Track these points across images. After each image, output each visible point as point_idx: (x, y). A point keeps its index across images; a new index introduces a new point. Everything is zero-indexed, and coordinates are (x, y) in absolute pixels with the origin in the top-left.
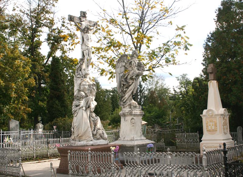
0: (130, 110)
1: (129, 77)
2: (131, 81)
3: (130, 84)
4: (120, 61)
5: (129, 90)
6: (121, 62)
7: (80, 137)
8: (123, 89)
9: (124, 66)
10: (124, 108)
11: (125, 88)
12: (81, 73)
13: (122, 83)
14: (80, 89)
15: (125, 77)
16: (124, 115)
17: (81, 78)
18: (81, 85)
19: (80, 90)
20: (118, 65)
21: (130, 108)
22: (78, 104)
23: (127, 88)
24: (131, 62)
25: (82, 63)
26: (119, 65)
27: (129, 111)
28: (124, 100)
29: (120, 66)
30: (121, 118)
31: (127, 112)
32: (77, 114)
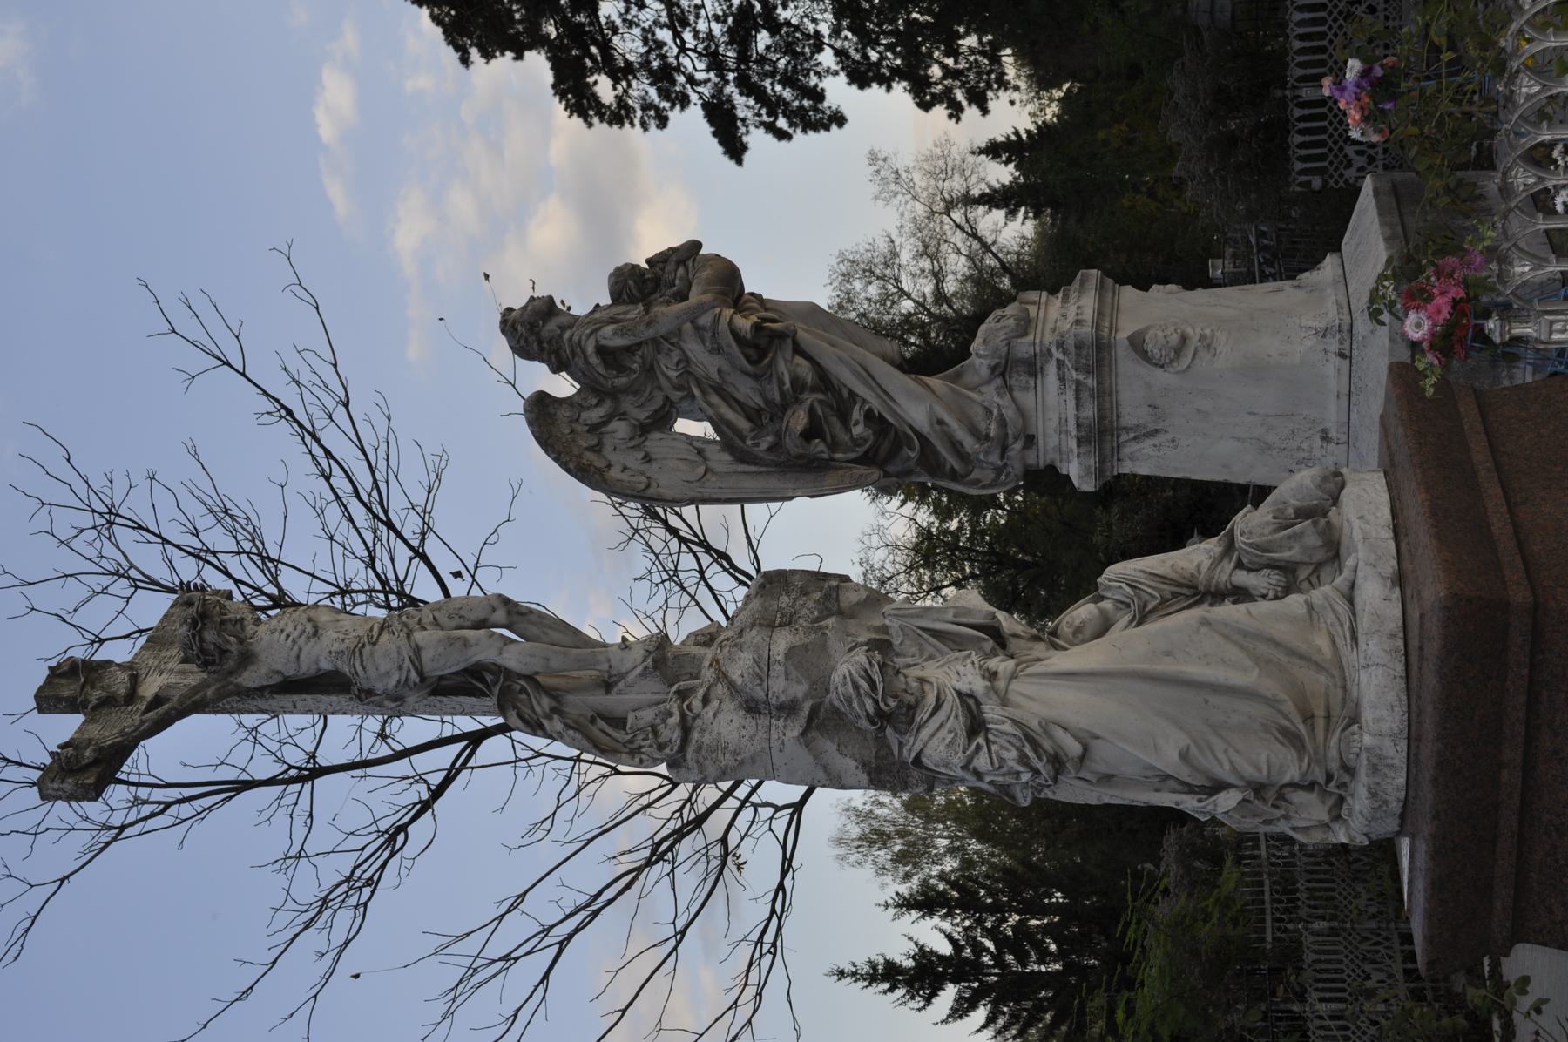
0: (1051, 369)
1: (746, 389)
2: (782, 366)
3: (804, 369)
4: (590, 456)
5: (861, 390)
6: (597, 449)
7: (1308, 718)
8: (856, 442)
9: (644, 429)
10: (1030, 440)
11: (849, 431)
12: (648, 715)
13: (792, 444)
14: (806, 711)
15: (743, 424)
16: (1101, 434)
17: (696, 704)
18: (760, 693)
19: (814, 711)
20: (625, 477)
21: (1033, 367)
22: (958, 723)
23: (843, 403)
24: (601, 351)
25: (546, 702)
26: (625, 468)
27: (1062, 379)
28: (956, 447)
29: (634, 460)
30: (1127, 468)
31: (1072, 404)
32: (1059, 733)
